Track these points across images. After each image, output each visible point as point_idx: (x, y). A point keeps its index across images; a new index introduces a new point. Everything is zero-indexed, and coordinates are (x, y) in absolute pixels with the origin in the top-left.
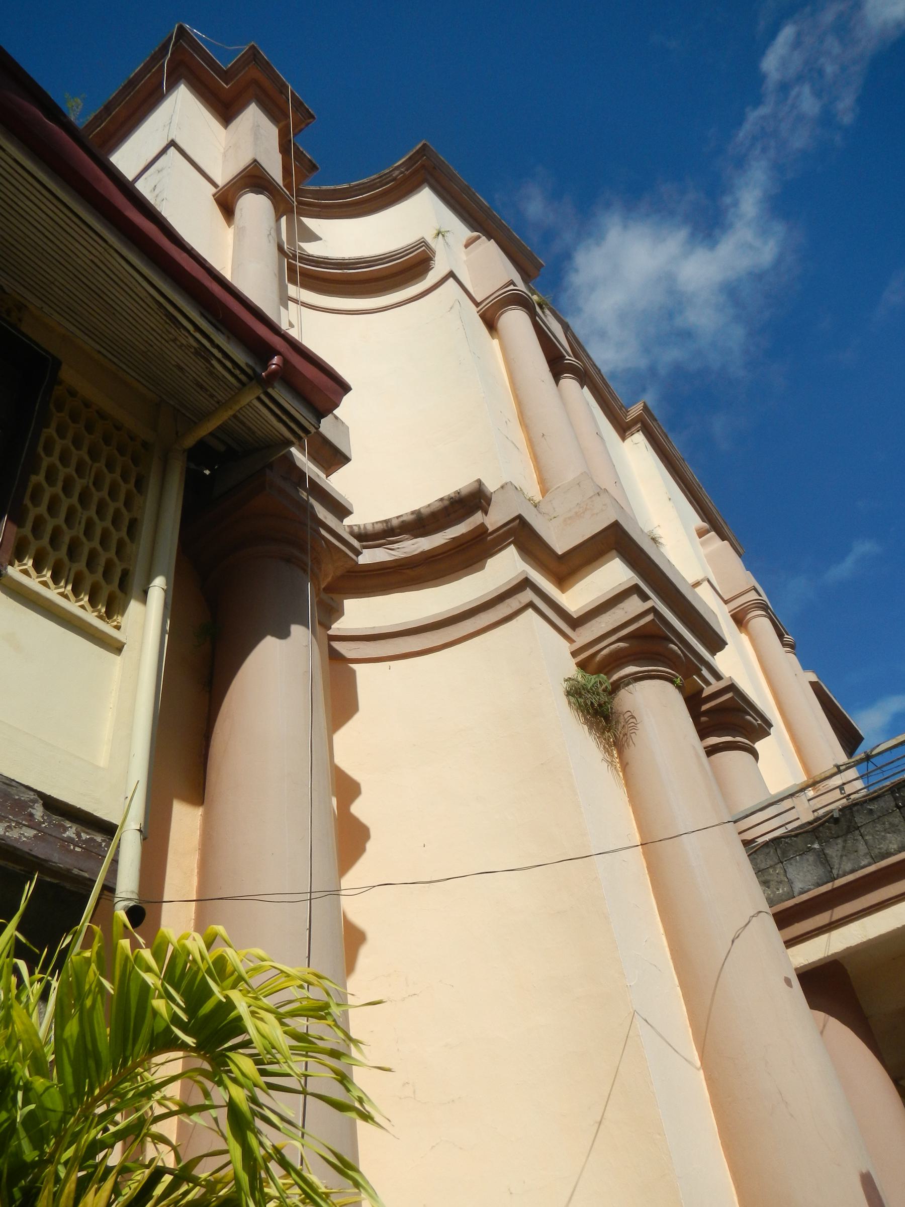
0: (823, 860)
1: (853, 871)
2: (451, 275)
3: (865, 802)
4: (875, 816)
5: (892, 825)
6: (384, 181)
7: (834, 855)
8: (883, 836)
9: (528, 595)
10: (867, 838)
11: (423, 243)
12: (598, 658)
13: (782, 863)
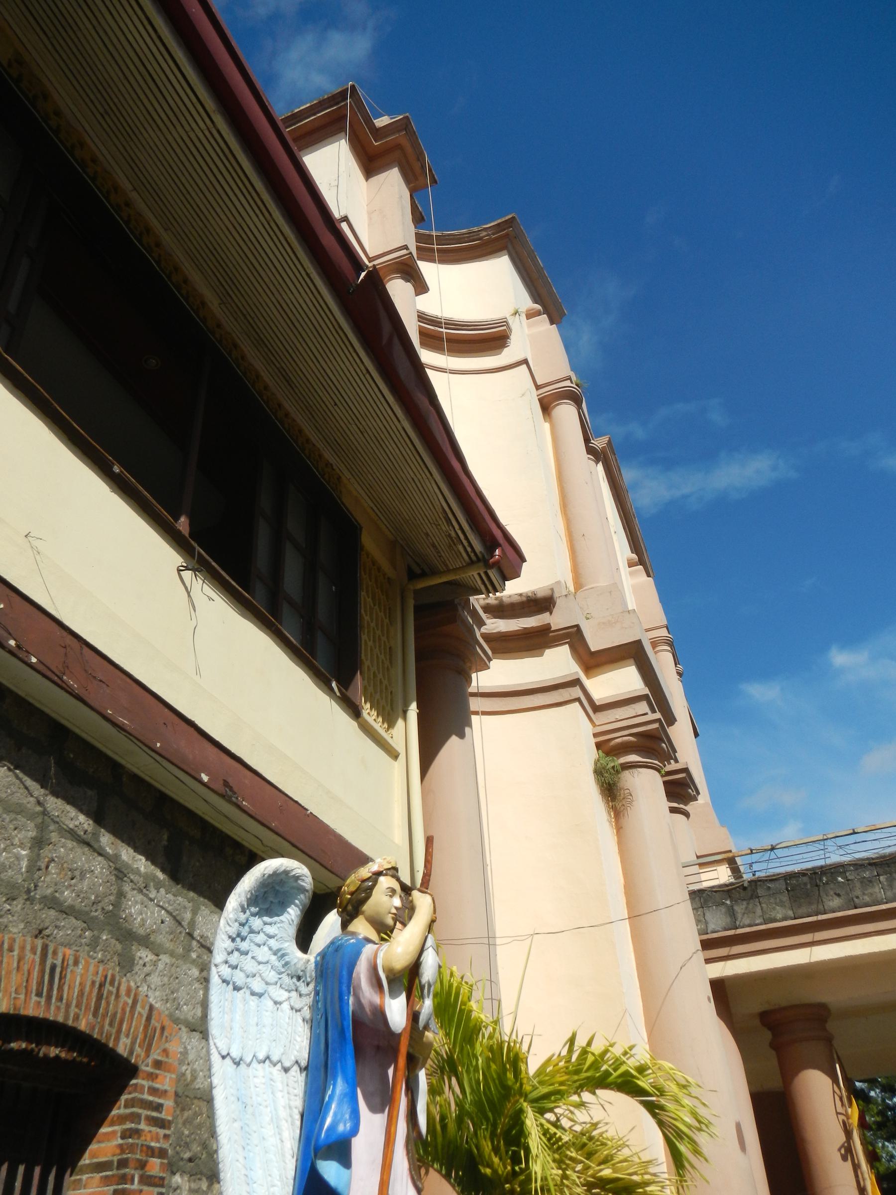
0: (732, 913)
1: (750, 926)
2: (525, 362)
3: (766, 880)
4: (771, 892)
5: (781, 901)
6: (472, 238)
7: (739, 911)
8: (774, 907)
9: (576, 692)
10: (763, 905)
11: (504, 322)
12: (613, 743)
13: (703, 908)
